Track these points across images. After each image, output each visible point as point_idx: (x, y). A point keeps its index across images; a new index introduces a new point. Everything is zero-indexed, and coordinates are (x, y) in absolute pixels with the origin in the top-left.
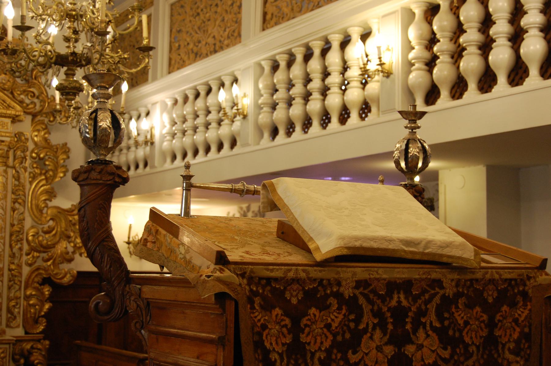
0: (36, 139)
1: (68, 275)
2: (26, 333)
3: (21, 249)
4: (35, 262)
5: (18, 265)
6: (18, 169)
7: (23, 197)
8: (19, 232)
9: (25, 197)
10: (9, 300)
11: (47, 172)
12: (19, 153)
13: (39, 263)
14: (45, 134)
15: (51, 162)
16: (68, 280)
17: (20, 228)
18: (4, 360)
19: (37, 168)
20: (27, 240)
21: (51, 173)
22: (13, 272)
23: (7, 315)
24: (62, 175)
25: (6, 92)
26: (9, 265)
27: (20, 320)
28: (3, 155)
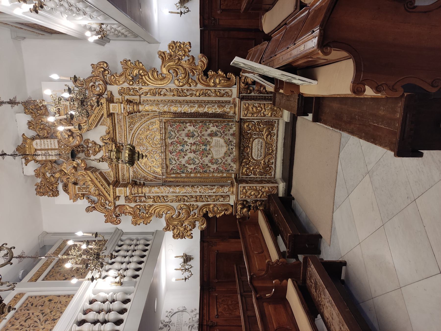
0: (121, 82)
1: (202, 59)
2: (235, 84)
4: (195, 81)
5: (197, 92)
7: (157, 90)
10: (216, 96)
11: (140, 75)
12: (131, 93)
13: (196, 78)
14: (117, 76)
15: (134, 72)
16: (205, 60)
17: (175, 91)
19: (138, 81)
20: (182, 86)
21: (141, 71)
24: (141, 65)
25: (93, 109)
27: (227, 89)
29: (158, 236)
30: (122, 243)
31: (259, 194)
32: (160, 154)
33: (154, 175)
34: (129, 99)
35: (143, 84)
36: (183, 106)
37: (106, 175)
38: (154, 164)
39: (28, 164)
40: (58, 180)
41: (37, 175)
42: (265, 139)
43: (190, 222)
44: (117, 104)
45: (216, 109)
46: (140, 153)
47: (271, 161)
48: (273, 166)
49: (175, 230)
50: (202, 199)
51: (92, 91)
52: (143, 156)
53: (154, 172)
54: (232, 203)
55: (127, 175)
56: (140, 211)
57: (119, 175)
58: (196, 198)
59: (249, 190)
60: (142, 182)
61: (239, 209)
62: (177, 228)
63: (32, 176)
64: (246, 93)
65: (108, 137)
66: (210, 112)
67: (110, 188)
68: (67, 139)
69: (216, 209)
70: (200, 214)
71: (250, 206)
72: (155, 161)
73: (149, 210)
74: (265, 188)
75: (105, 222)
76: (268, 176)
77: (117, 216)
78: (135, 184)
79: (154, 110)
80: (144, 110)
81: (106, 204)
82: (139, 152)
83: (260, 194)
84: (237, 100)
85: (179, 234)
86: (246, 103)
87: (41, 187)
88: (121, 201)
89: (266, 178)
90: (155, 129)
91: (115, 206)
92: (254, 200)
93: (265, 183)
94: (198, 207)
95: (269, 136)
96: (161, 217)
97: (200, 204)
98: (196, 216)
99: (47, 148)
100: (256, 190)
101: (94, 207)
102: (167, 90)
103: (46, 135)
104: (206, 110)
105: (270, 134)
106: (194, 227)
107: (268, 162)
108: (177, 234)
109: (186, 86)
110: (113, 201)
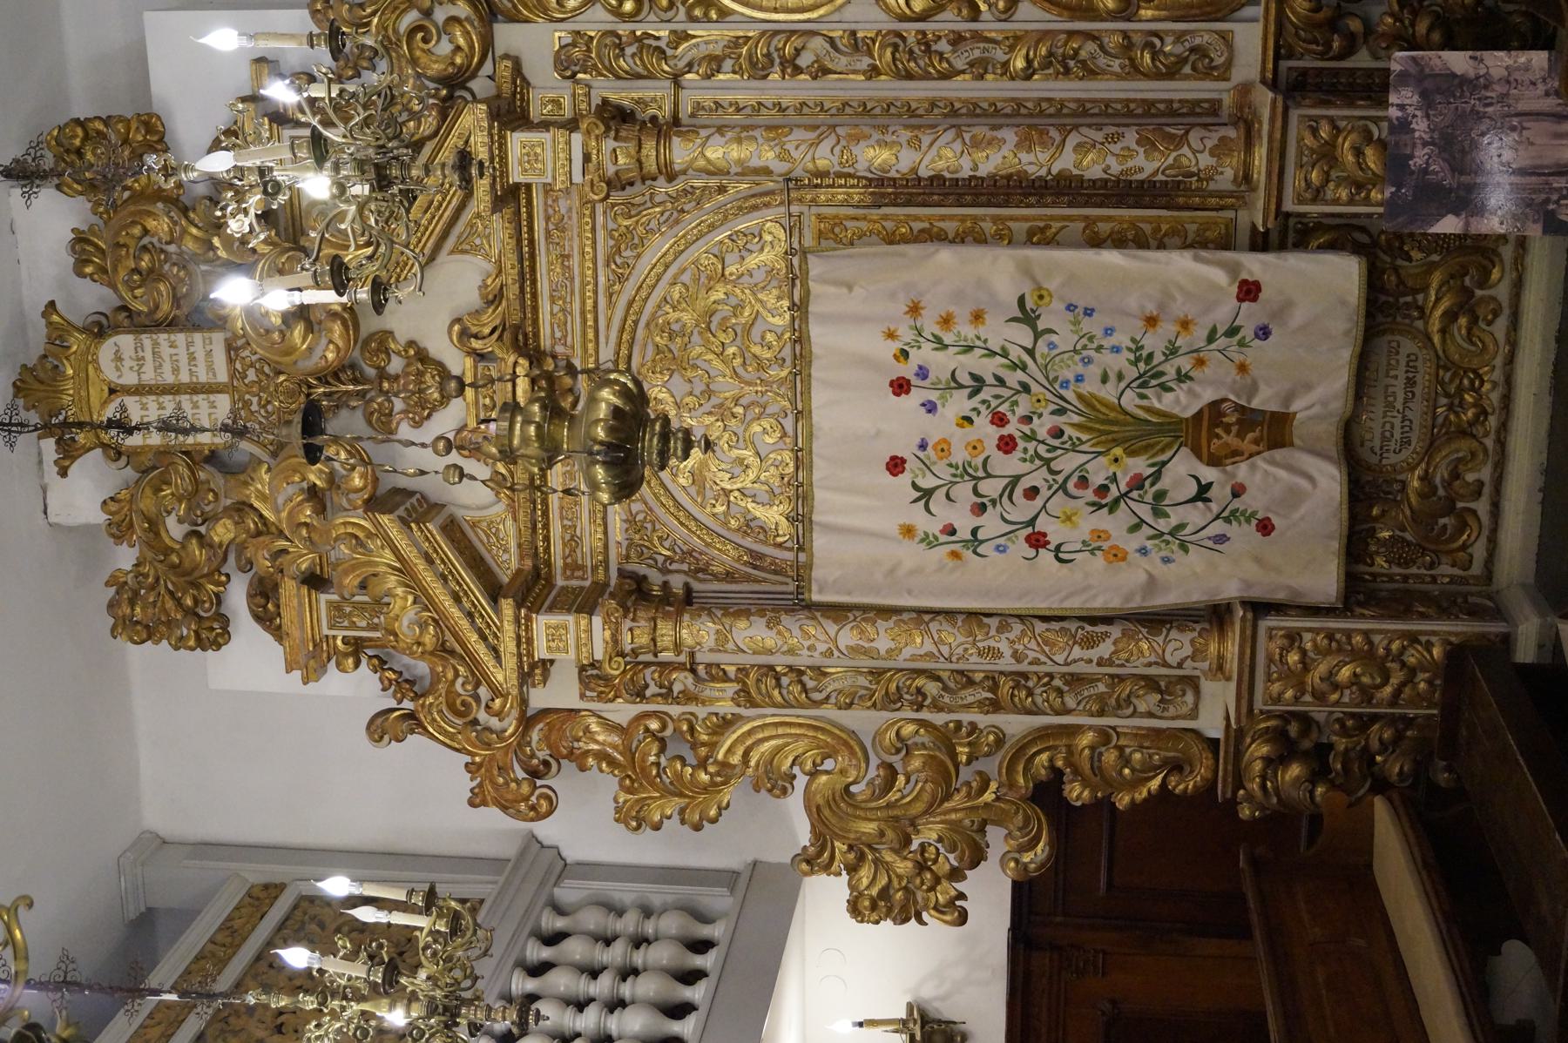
3: (957, 40)
5: (1012, 48)
6: (681, 64)
7: (778, 42)
8: (896, 47)
9: (776, 33)
10: (1135, 71)
17: (882, 47)
18: (1342, 124)
20: (923, 17)
22: (1036, 64)
23: (1187, 77)
26: (1012, 79)
27: (1204, 32)
28: (633, 152)
29: (766, 896)
30: (560, 923)
31: (1386, 682)
32: (788, 423)
33: (748, 542)
34: (613, 97)
35: (698, 12)
36: (926, 140)
37: (478, 539)
38: (746, 481)
39: (74, 470)
40: (225, 559)
41: (119, 530)
42: (1436, 339)
43: (955, 826)
44: (545, 137)
45: (1128, 153)
46: (675, 424)
47: (1470, 477)
48: (1482, 507)
49: (865, 874)
50: (1030, 693)
51: (414, 62)
52: (688, 445)
53: (750, 526)
54: (1212, 724)
55: (591, 538)
56: (662, 750)
57: (547, 539)
58: (994, 688)
59: (1328, 652)
60: (677, 583)
61: (1258, 766)
62: (876, 862)
63: (87, 530)
64: (1322, 56)
65: (490, 319)
66: (1095, 172)
67: (498, 611)
68: (276, 336)
69: (1110, 757)
70: (1012, 785)
71: (1323, 750)
72: (751, 459)
73: (713, 746)
74: (1428, 646)
75: (472, 804)
76: (1445, 569)
77: (534, 774)
78: (636, 593)
79: (755, 163)
80: (701, 163)
81: (477, 698)
82: (666, 421)
83: (1394, 681)
84: (1264, 99)
85: (885, 893)
86: (1316, 119)
87: (136, 593)
88: (559, 692)
89: (1434, 579)
90: (759, 276)
91: (523, 713)
92: (1353, 715)
93: (1424, 616)
94: (1000, 741)
95: (1463, 321)
96: (784, 791)
97: (1015, 725)
98: (988, 796)
99: (169, 378)
100: (1367, 656)
101: (411, 716)
102: (831, 41)
103: (165, 307)
104: (1066, 161)
105: (1465, 305)
106: (977, 856)
107: (1448, 484)
108: (874, 892)
109: (949, 14)
110: (515, 692)
